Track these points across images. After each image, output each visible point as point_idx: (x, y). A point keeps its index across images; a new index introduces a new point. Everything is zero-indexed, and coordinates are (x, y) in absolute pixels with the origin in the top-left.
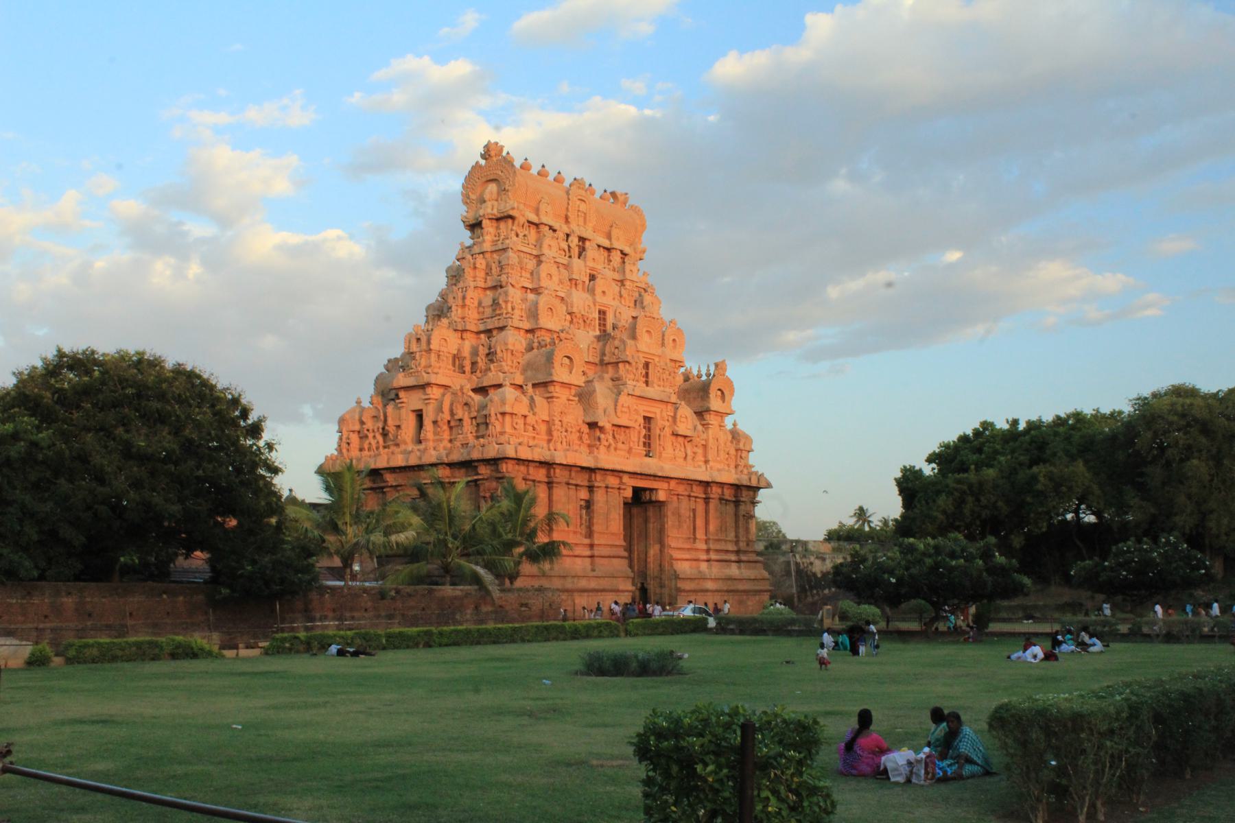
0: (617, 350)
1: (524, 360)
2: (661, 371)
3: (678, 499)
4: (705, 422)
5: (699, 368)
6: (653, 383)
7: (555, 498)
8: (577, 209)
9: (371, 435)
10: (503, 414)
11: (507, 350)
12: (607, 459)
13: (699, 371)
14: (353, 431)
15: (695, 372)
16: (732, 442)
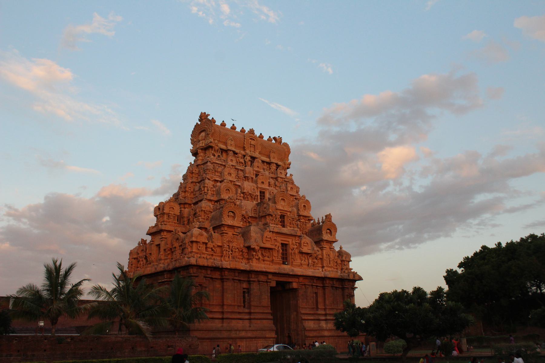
0: (265, 209)
1: (210, 216)
2: (291, 219)
3: (305, 287)
4: (320, 247)
5: (318, 219)
6: (287, 225)
7: (225, 287)
8: (249, 143)
9: (141, 259)
10: (192, 242)
11: (202, 210)
12: (257, 266)
13: (318, 221)
14: (135, 259)
15: (317, 221)
16: (338, 256)
